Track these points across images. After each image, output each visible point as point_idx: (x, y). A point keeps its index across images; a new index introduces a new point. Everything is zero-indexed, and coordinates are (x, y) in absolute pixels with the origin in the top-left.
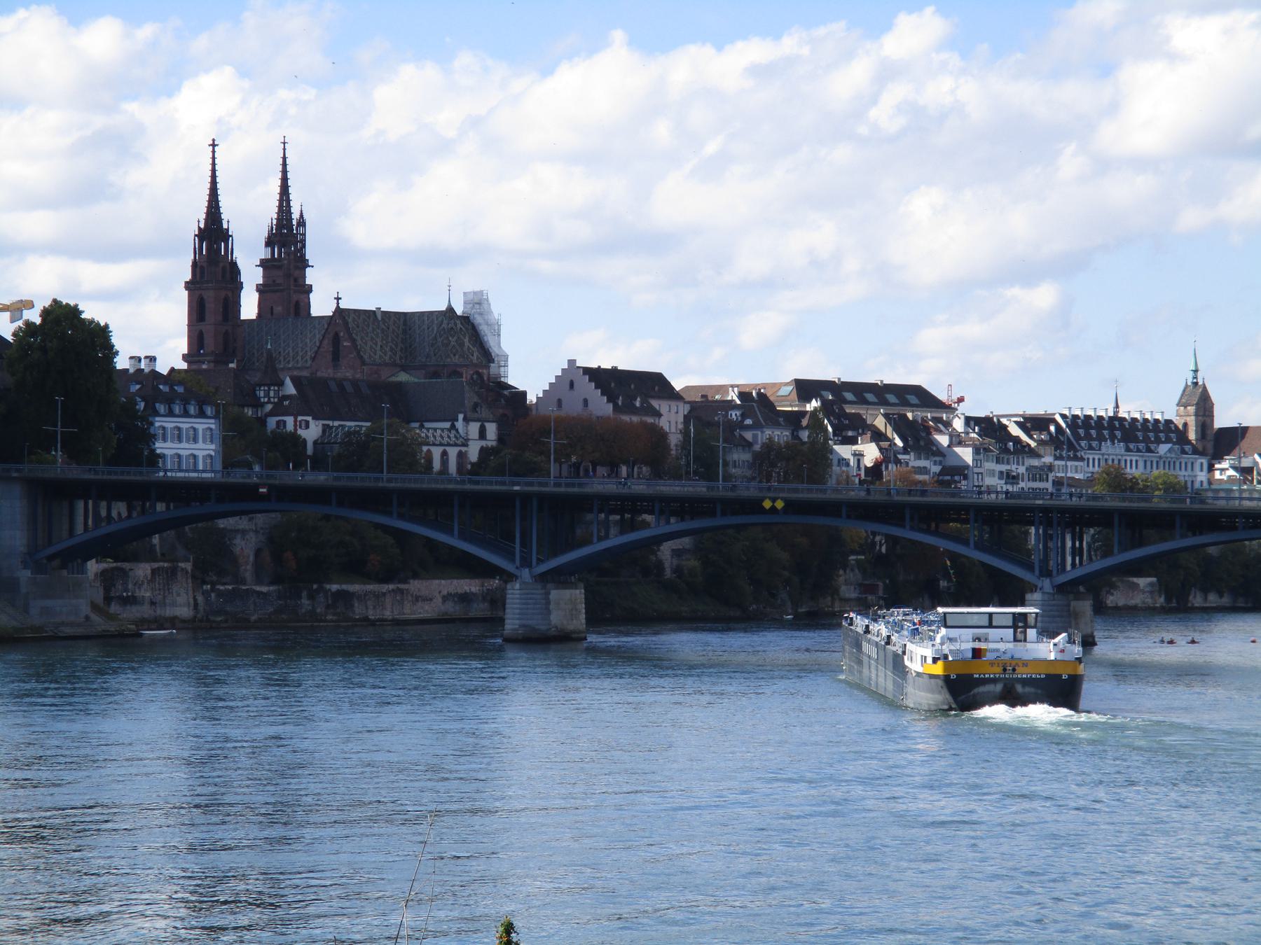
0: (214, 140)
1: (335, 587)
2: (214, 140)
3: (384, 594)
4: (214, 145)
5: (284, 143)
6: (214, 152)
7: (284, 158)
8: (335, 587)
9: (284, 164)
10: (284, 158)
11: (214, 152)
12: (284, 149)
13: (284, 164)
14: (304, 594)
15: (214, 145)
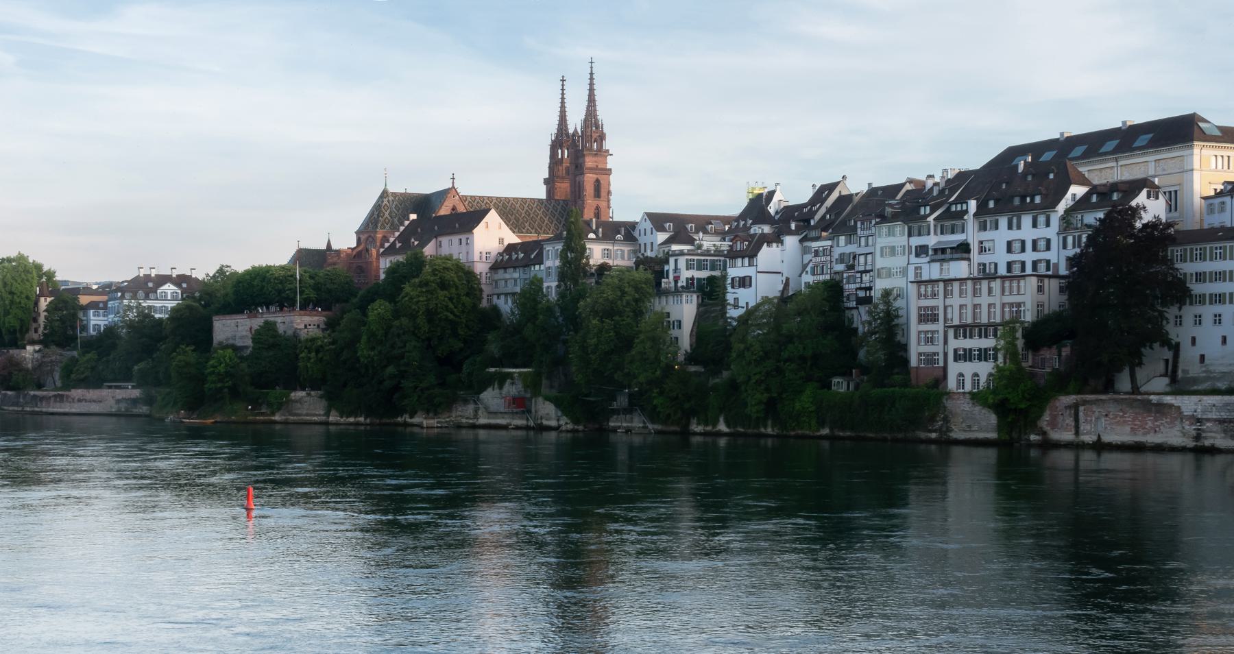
0: (563, 77)
1: (32, 393)
2: (563, 77)
3: (50, 397)
4: (563, 81)
5: (592, 63)
6: (563, 85)
7: (591, 74)
8: (32, 393)
9: (591, 79)
10: (591, 74)
11: (563, 85)
12: (591, 67)
13: (591, 79)
14: (21, 396)
15: (563, 81)
